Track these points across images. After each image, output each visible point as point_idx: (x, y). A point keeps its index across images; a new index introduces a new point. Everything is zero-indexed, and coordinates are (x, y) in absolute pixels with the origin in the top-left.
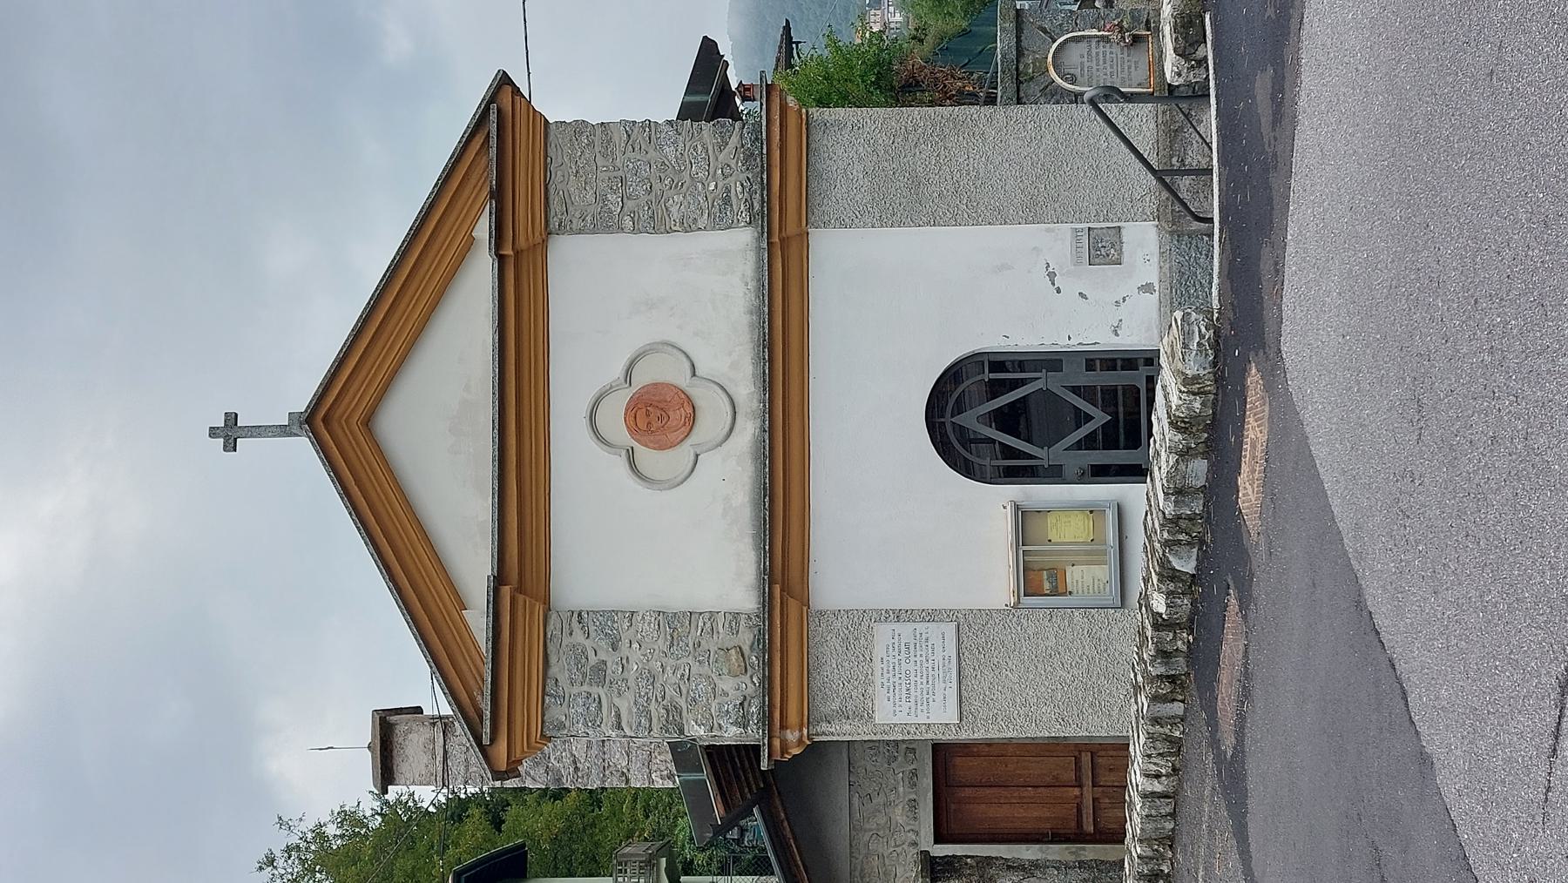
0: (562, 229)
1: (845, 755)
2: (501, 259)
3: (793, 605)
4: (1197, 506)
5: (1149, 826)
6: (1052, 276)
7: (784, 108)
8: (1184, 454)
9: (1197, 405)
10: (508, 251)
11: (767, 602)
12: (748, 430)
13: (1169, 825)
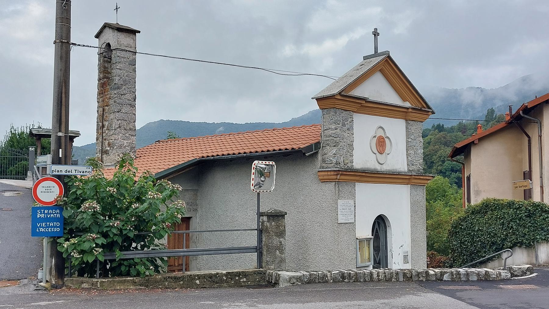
0: (407, 123)
1: (190, 188)
2: (408, 108)
3: (407, 181)
4: (464, 279)
5: (362, 275)
6: (402, 246)
7: (429, 180)
8: (478, 274)
9: (494, 276)
10: (410, 110)
11: (356, 171)
12: (379, 168)
13: (362, 280)
